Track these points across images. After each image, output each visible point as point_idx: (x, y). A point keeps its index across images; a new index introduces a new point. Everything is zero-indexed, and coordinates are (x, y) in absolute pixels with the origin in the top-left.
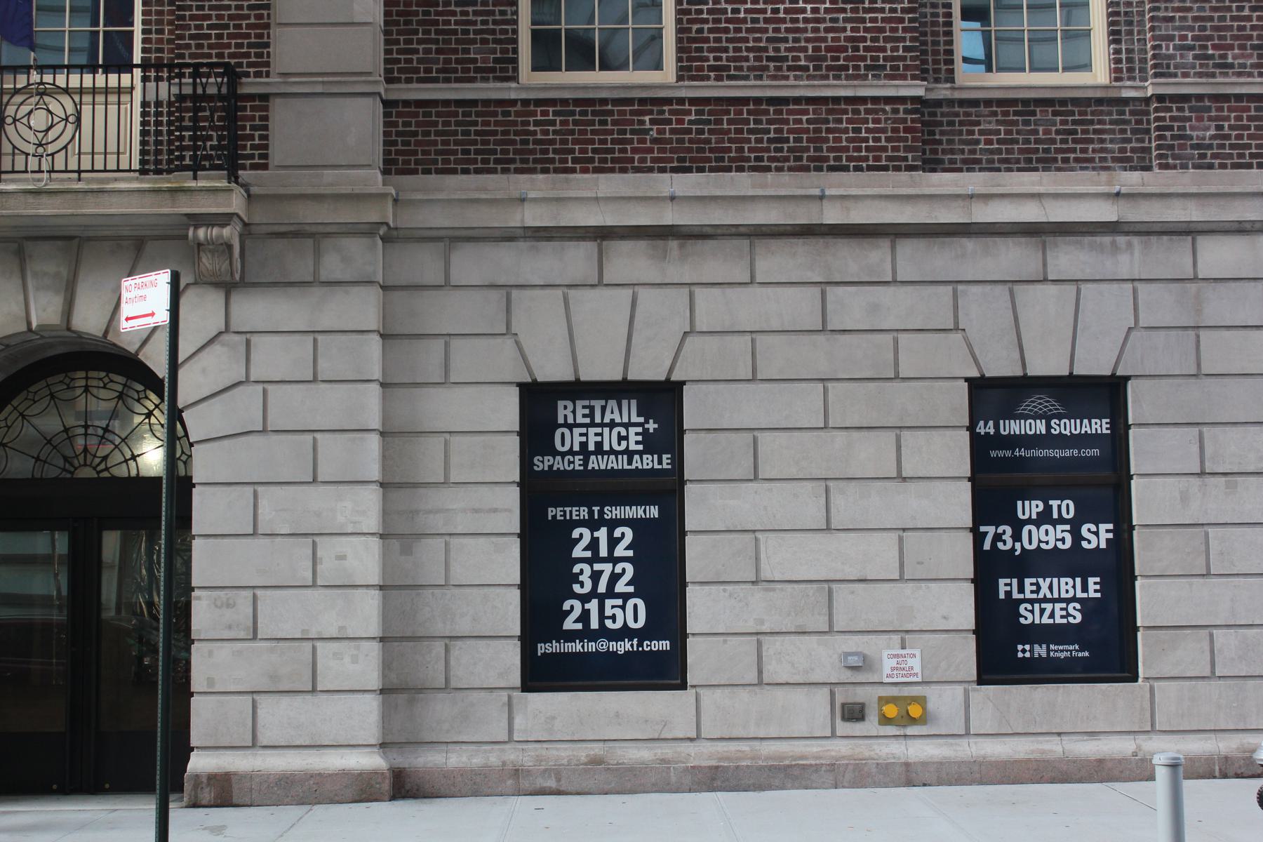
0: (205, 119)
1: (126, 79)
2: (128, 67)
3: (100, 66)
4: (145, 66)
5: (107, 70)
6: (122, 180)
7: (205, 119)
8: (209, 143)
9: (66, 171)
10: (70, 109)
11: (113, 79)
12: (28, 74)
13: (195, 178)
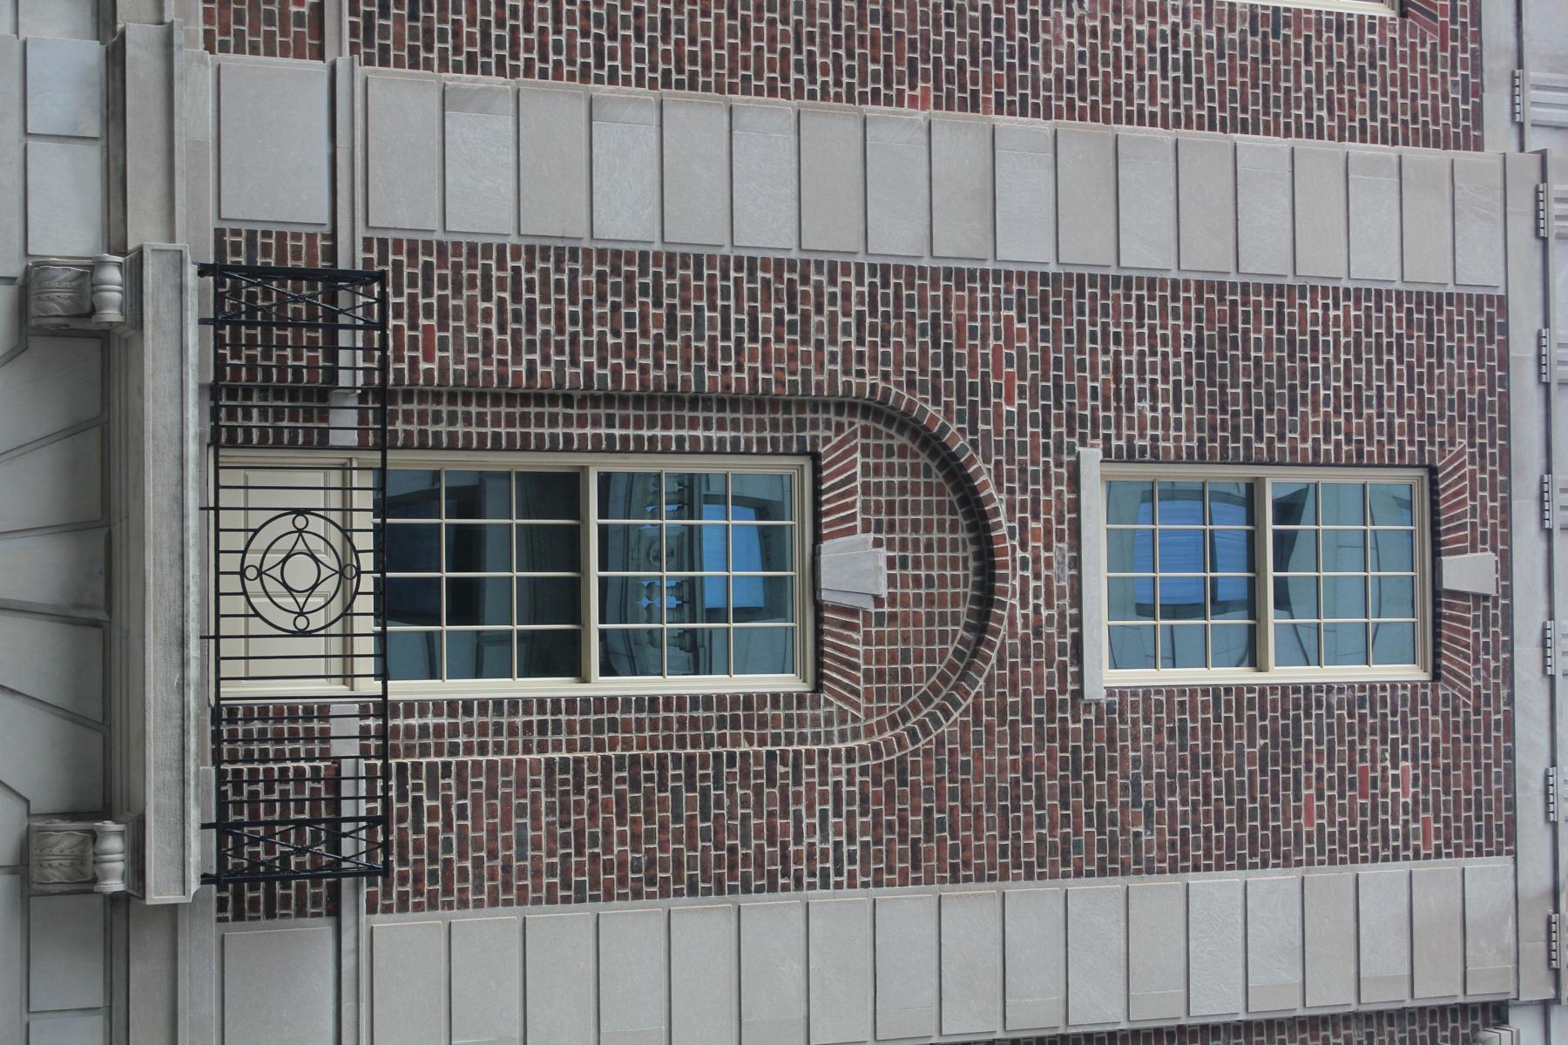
0: (297, 289)
1: (366, 666)
2: (383, 675)
3: (384, 521)
4: (384, 707)
5: (378, 531)
6: (204, 667)
7: (297, 289)
8: (263, 857)
9: (218, 616)
10: (317, 621)
11: (366, 645)
12: (376, 676)
13: (204, 826)
